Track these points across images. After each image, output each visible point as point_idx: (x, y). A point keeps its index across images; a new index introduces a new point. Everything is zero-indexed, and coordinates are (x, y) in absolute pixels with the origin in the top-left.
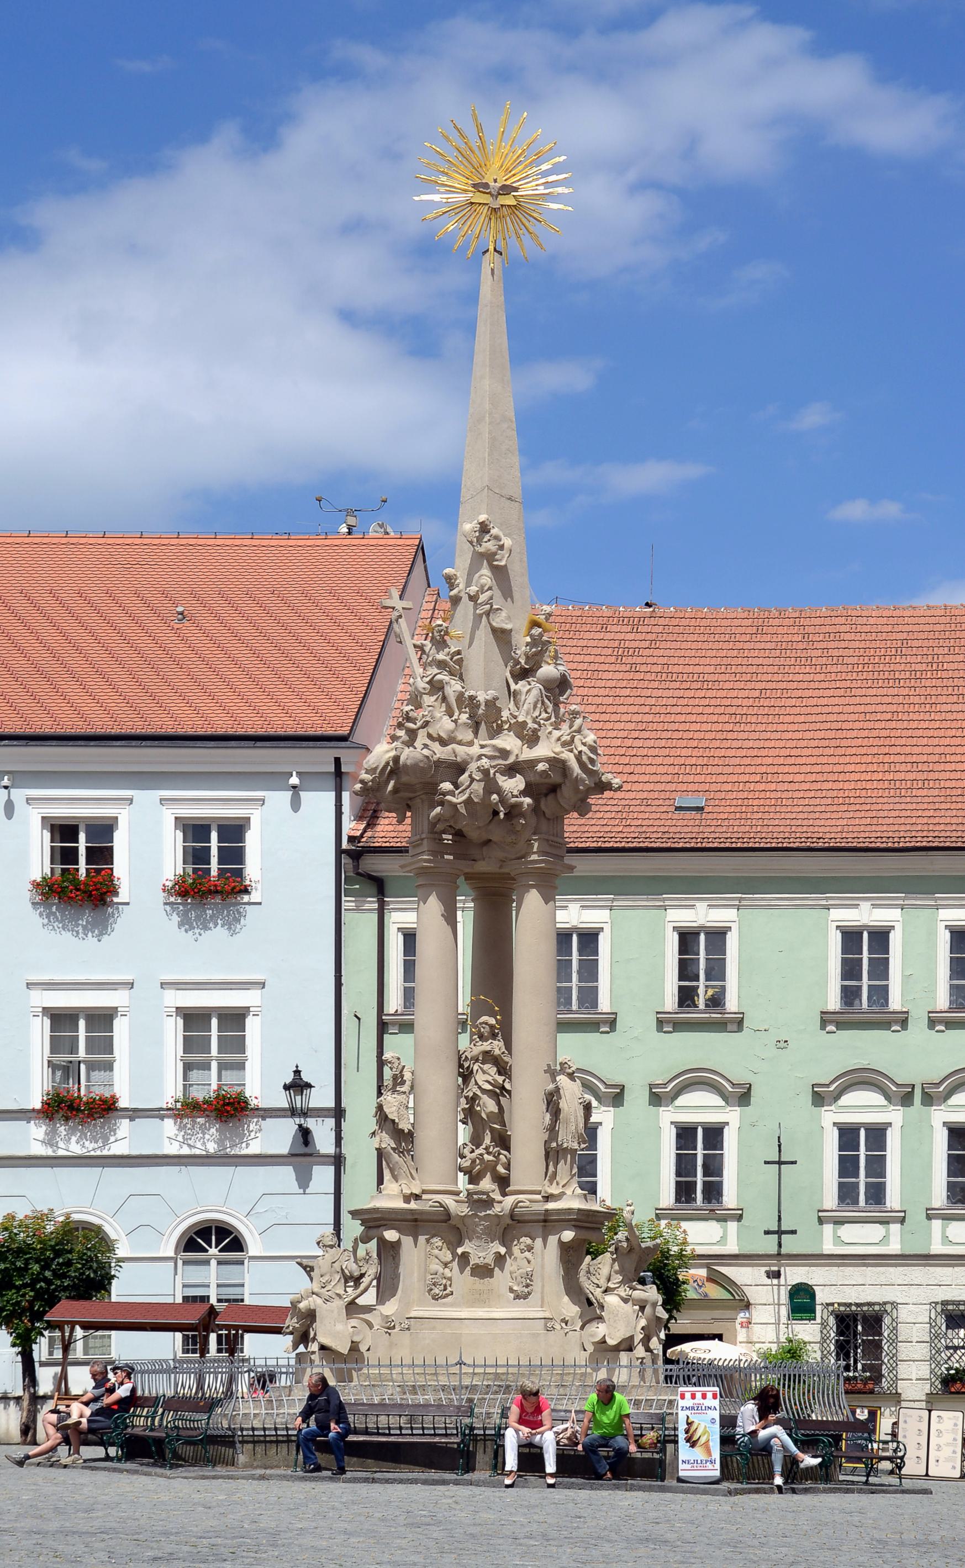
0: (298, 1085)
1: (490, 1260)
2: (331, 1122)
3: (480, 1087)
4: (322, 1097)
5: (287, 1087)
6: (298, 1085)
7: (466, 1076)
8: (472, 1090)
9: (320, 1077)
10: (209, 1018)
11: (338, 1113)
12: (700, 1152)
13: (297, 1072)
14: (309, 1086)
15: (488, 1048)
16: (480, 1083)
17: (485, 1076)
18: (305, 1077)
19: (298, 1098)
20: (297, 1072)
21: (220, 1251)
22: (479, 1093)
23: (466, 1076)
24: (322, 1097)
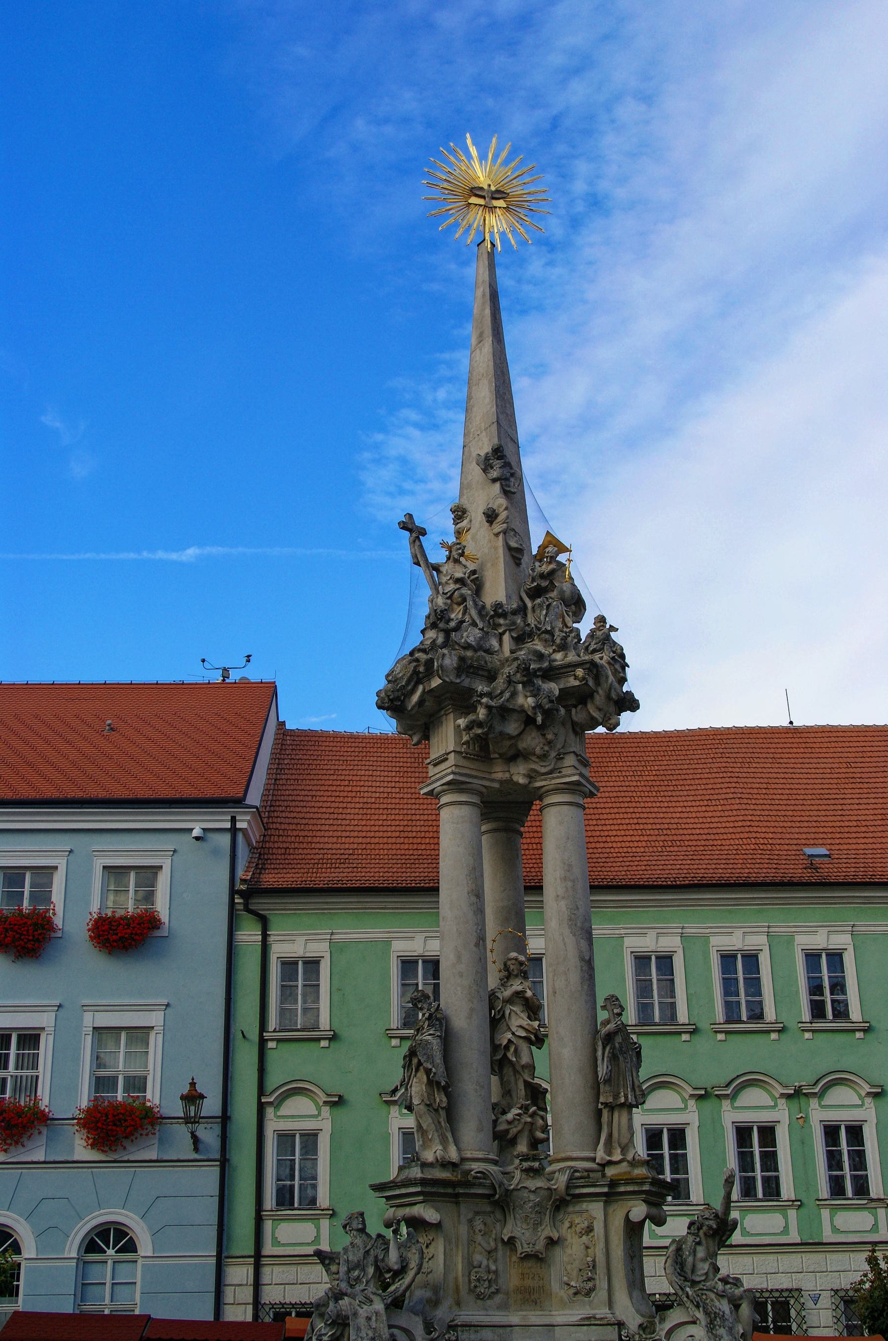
0: (193, 1097)
1: (540, 1246)
2: (217, 1129)
3: (513, 1034)
5: (183, 1098)
6: (193, 1097)
7: (496, 1022)
8: (504, 1038)
11: (225, 1119)
14: (202, 1097)
15: (520, 988)
16: (514, 1029)
17: (518, 1020)
19: (192, 1108)
21: (116, 1252)
22: (513, 1039)
23: (496, 1022)
24: (211, 1105)
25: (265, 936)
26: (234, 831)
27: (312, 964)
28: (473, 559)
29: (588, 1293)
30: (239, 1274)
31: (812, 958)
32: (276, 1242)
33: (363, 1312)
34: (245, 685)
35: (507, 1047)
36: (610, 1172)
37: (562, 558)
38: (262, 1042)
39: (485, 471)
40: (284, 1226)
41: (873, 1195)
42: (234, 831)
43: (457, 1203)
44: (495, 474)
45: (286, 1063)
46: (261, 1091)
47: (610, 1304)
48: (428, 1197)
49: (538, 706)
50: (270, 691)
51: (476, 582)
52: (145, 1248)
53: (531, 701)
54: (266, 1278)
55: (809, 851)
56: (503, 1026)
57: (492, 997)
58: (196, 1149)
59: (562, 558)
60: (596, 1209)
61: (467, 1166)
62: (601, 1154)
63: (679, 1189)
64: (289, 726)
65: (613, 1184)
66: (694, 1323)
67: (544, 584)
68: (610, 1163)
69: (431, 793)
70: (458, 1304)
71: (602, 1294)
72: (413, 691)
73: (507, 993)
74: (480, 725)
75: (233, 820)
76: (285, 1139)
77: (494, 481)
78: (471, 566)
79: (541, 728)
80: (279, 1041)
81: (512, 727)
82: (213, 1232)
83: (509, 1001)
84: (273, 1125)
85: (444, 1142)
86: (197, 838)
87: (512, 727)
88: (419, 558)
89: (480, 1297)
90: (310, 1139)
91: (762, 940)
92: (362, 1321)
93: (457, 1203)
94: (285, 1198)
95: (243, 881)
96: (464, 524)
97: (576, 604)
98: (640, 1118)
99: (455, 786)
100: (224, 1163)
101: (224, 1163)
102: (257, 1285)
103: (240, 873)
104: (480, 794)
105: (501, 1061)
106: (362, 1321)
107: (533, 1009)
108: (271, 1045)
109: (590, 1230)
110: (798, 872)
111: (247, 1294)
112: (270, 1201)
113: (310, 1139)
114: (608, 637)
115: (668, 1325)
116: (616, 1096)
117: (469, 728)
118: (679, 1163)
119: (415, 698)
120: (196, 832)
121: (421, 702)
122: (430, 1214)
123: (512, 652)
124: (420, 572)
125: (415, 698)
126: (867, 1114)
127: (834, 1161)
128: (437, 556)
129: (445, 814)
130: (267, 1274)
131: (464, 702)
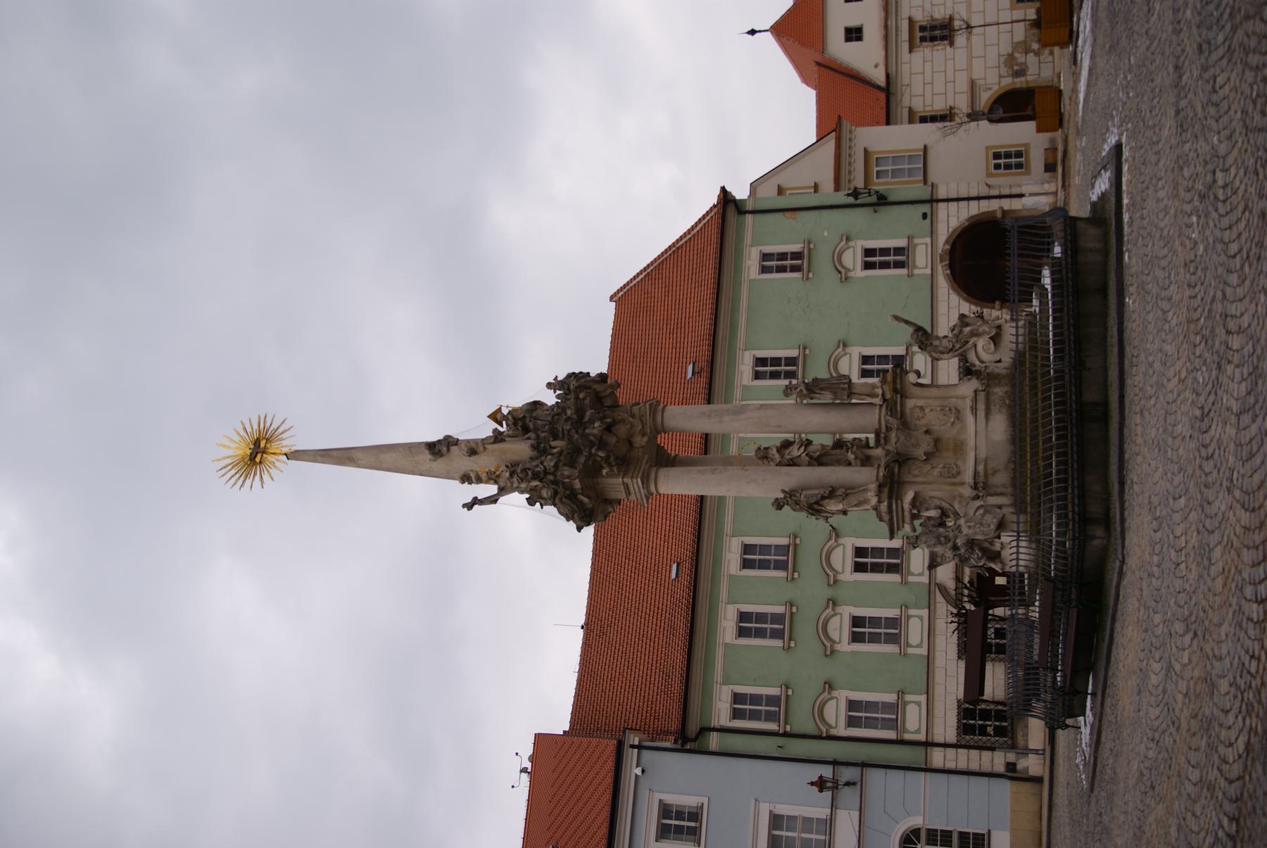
4: (827, 771)
6: (821, 784)
8: (805, 458)
9: (815, 772)
10: (774, 836)
11: (835, 763)
12: (868, 560)
13: (812, 784)
14: (821, 777)
17: (795, 451)
18: (815, 779)
20: (812, 784)
23: (793, 463)
24: (827, 771)
25: (714, 729)
26: (640, 747)
27: (737, 698)
28: (498, 467)
29: (958, 411)
30: (938, 758)
31: (758, 376)
32: (918, 731)
33: (965, 531)
34: (531, 759)
35: (811, 457)
36: (888, 396)
37: (505, 411)
38: (786, 735)
39: (442, 455)
40: (913, 569)
41: (904, 353)
42: (640, 747)
43: (904, 483)
44: (445, 449)
45: (802, 721)
46: (819, 737)
47: (964, 398)
48: (899, 498)
49: (601, 419)
50: (540, 739)
51: (513, 468)
52: (917, 821)
53: (597, 425)
54: (941, 740)
55: (690, 374)
56: (797, 461)
57: (779, 464)
58: (854, 784)
59: (505, 411)
60: (910, 403)
61: (881, 479)
62: (878, 401)
63: (899, 361)
64: (567, 729)
65: (895, 391)
66: (975, 346)
67: (520, 423)
68: (883, 395)
69: (647, 498)
70: (962, 484)
71: (960, 403)
72: (581, 502)
73: (777, 456)
74: (608, 457)
75: (633, 746)
76: (852, 722)
77: (448, 450)
78: (503, 468)
79: (614, 423)
80: (786, 723)
81: (612, 440)
82: (910, 774)
83: (782, 456)
84: (842, 731)
85: (866, 490)
86: (643, 771)
87: (612, 440)
88: (493, 500)
89: (959, 473)
90: (853, 705)
91: (747, 353)
92: (971, 531)
93: (904, 483)
94: (892, 724)
95: (676, 742)
96: (472, 475)
97: (536, 405)
98: (855, 378)
99: (646, 481)
100: (864, 765)
101: (864, 765)
102: (945, 745)
103: (667, 745)
104: (651, 466)
105: (819, 460)
106: (971, 531)
107: (787, 444)
108: (788, 728)
109: (922, 408)
110: (703, 381)
111: (951, 752)
112: (891, 735)
113: (853, 705)
114: (562, 382)
115: (977, 363)
116: (844, 389)
117: (610, 465)
118: (883, 359)
119: (586, 500)
120: (638, 771)
121: (588, 497)
122: (909, 496)
123: (563, 439)
124: (502, 499)
125: (586, 500)
126: (856, 352)
127: (884, 265)
128: (492, 489)
129: (662, 490)
130: (939, 738)
131: (592, 471)
